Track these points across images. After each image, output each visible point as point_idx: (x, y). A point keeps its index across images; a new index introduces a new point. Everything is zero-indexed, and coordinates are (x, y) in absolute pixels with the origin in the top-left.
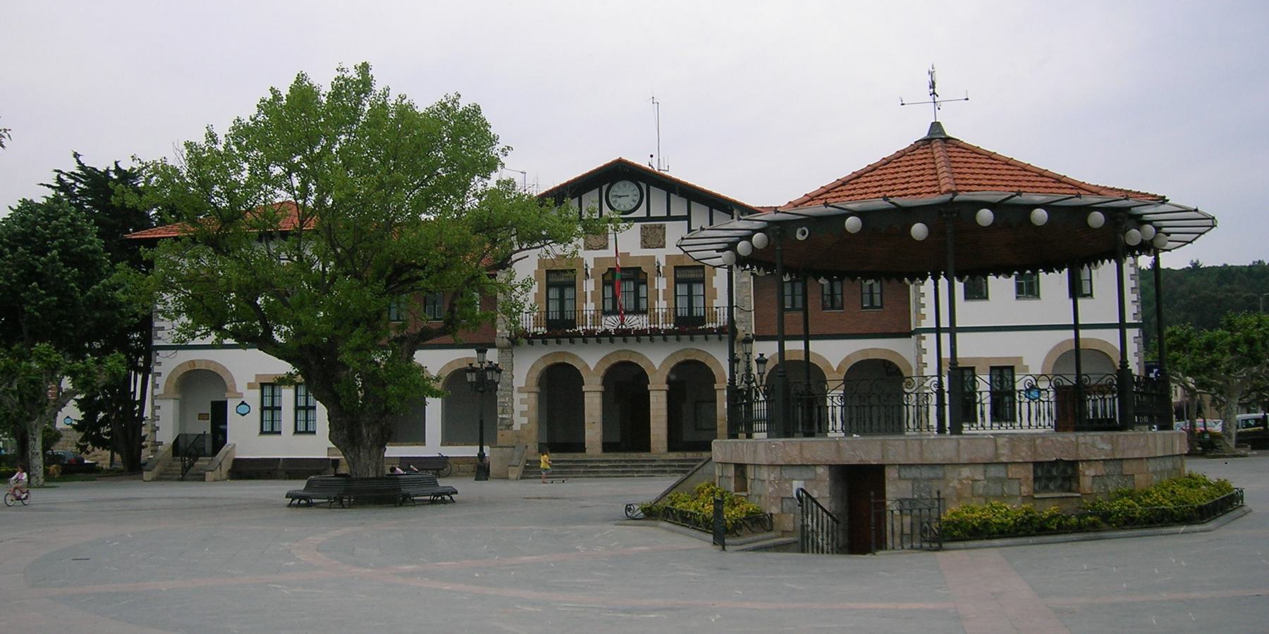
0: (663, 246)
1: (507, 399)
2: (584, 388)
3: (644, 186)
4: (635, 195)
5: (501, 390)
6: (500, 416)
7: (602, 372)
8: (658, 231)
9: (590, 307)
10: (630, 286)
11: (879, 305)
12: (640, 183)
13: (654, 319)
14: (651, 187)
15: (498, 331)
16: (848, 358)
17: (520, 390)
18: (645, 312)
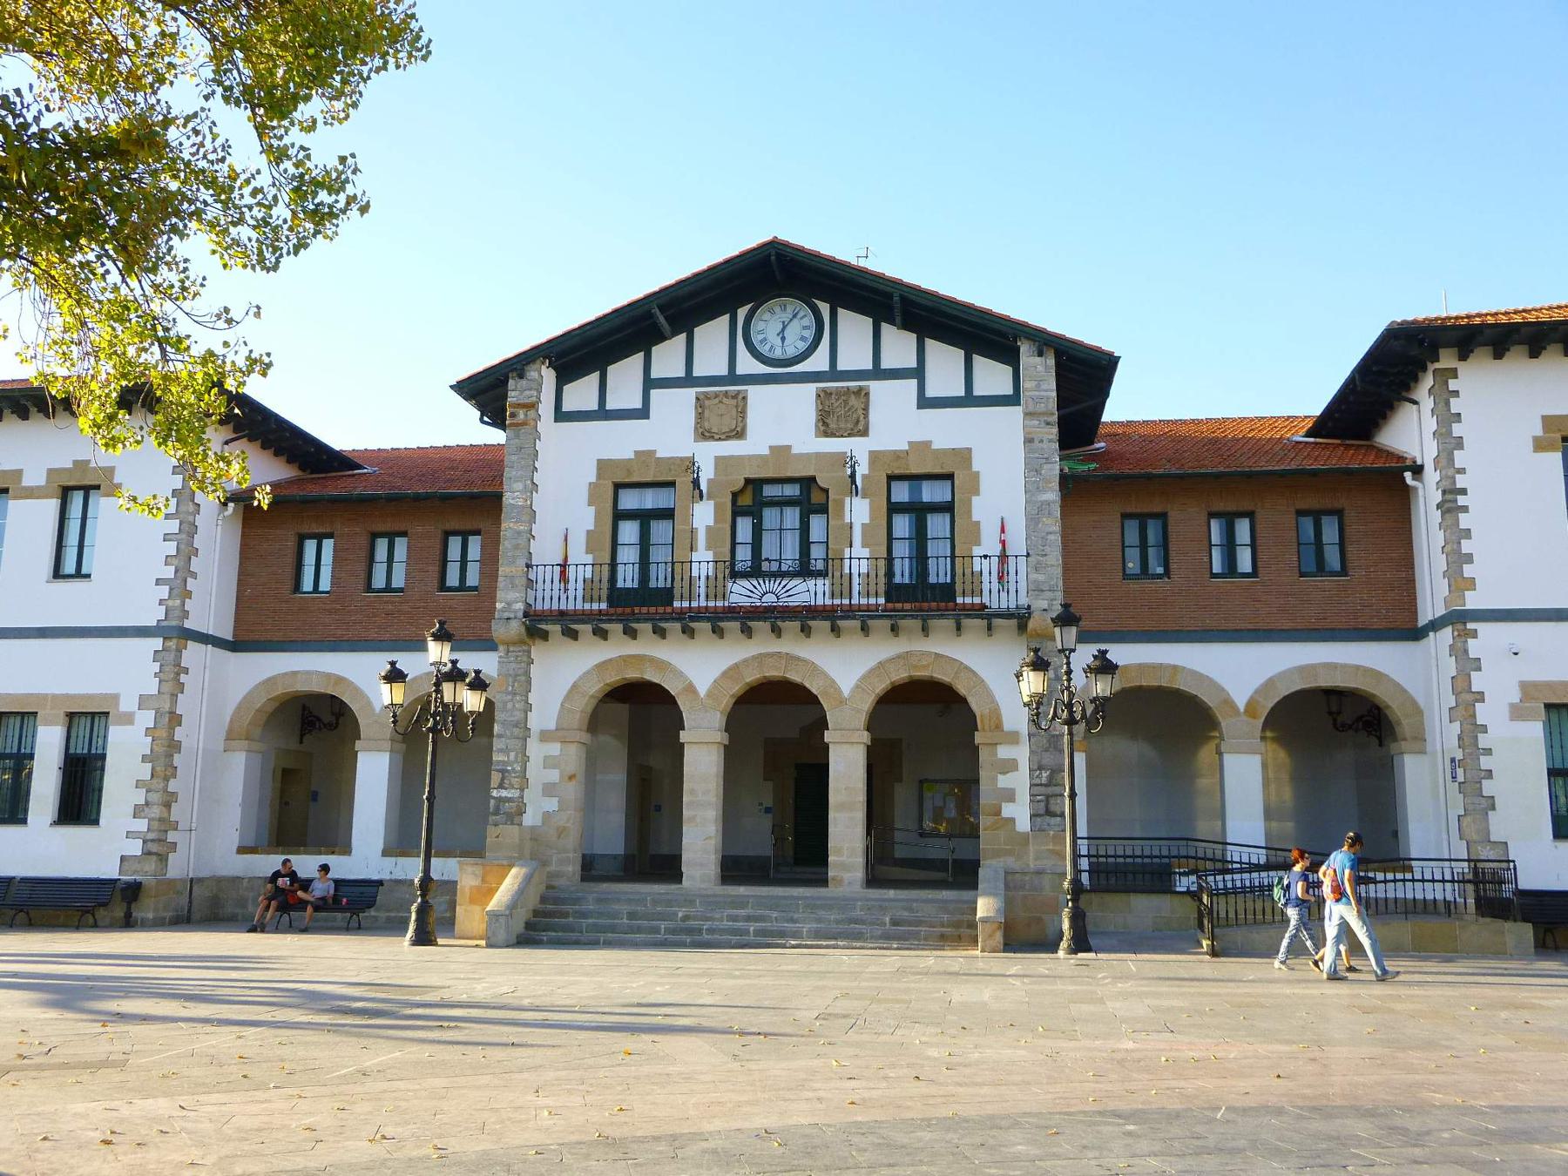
0: (864, 433)
1: (512, 755)
2: (684, 736)
3: (824, 308)
4: (805, 328)
5: (500, 736)
6: (495, 793)
7: (726, 702)
8: (853, 401)
9: (703, 561)
10: (792, 516)
11: (1249, 570)
12: (816, 301)
13: (843, 586)
14: (840, 310)
15: (499, 606)
16: (1270, 684)
17: (545, 736)
18: (823, 574)
